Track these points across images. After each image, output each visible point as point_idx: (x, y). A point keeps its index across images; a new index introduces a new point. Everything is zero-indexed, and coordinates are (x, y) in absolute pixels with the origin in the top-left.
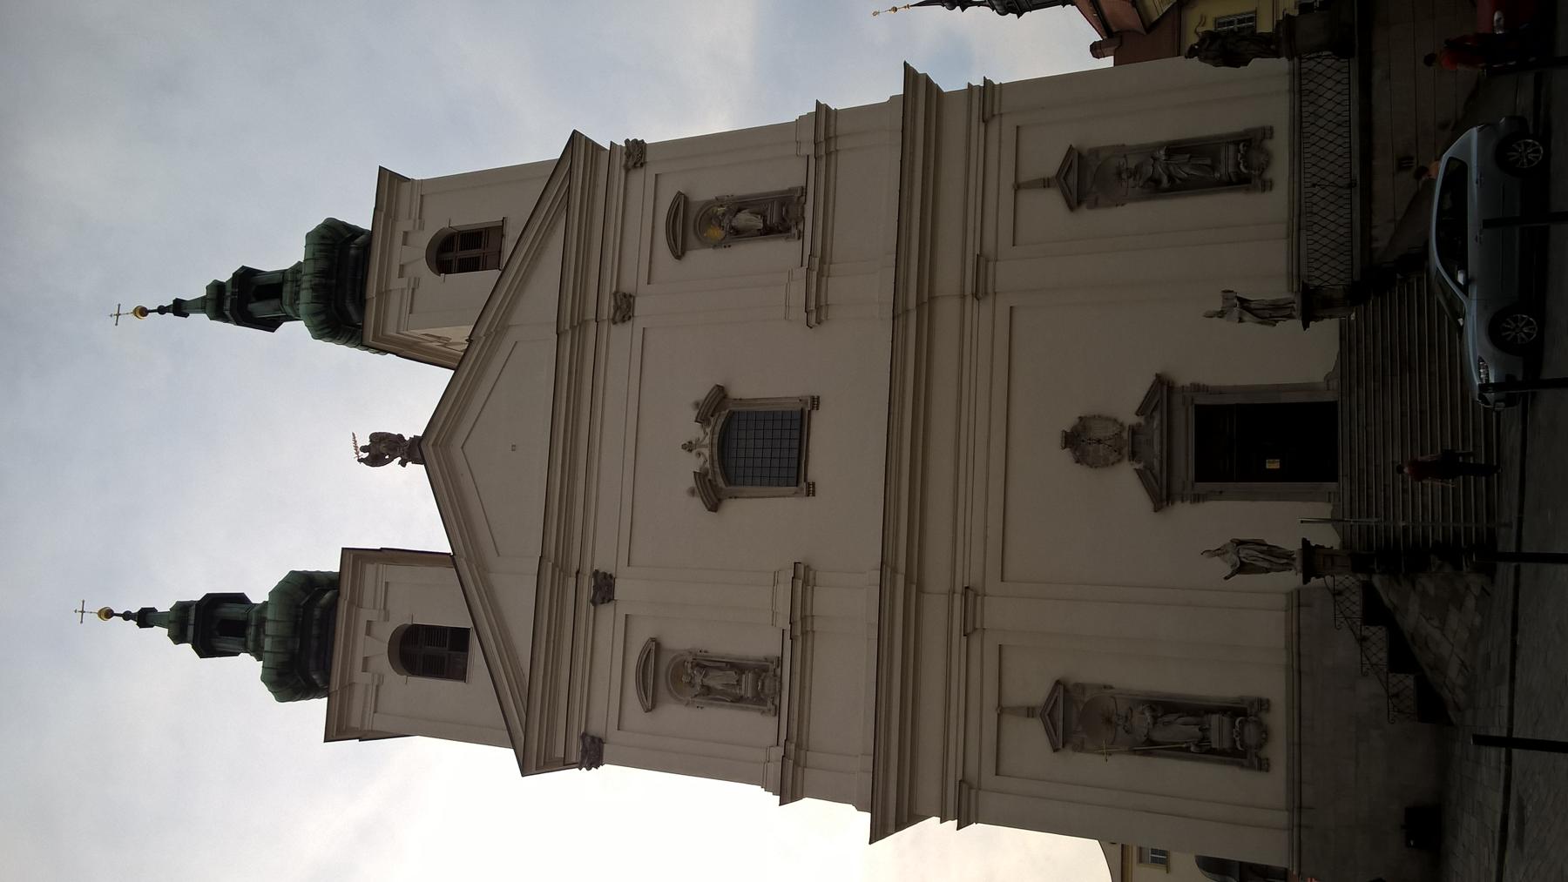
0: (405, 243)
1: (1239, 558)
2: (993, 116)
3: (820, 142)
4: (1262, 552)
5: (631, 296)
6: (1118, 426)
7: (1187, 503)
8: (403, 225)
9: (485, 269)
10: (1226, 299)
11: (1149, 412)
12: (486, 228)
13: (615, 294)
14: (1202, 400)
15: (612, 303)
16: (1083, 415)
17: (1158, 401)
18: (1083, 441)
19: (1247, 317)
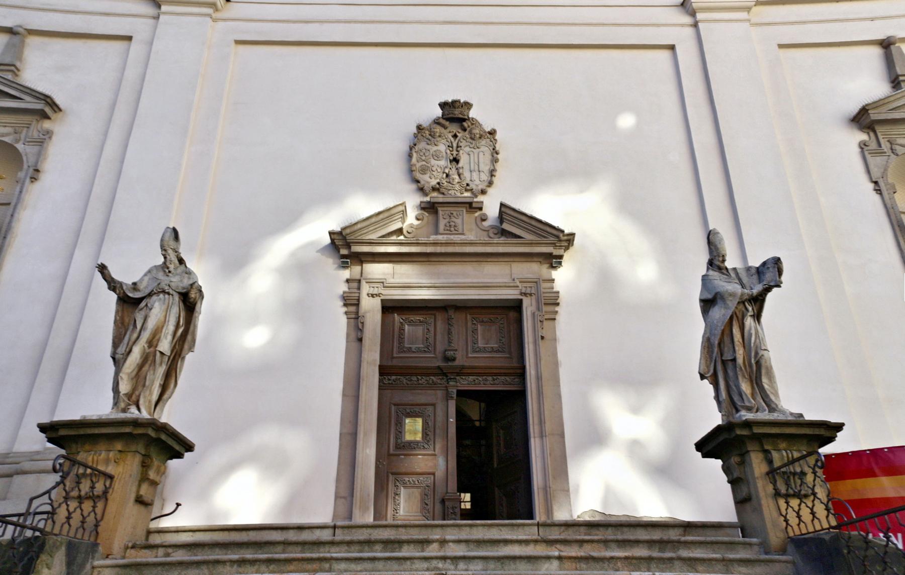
1: (150, 295)
4: (153, 342)
6: (480, 187)
7: (344, 288)
10: (760, 271)
11: (506, 226)
14: (528, 307)
16: (498, 136)
17: (519, 237)
18: (455, 136)
19: (719, 313)
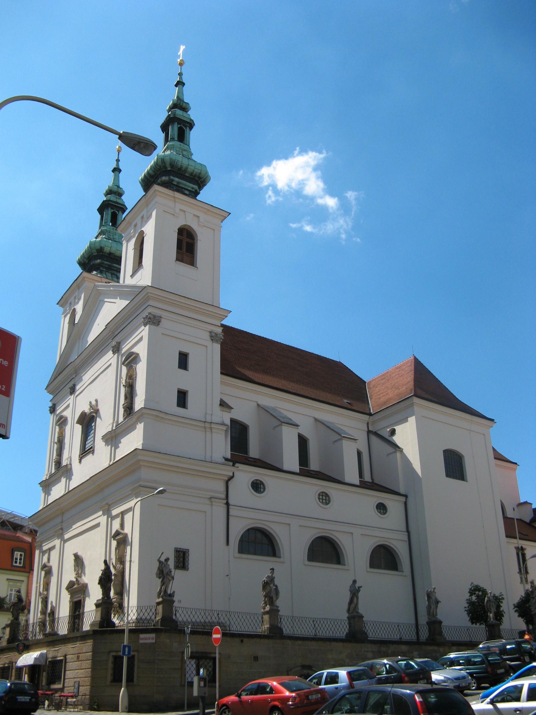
0: (194, 215)
2: (212, 502)
3: (211, 425)
5: (159, 325)
8: (203, 216)
9: (177, 252)
12: (194, 257)
13: (161, 317)
15: (157, 315)
